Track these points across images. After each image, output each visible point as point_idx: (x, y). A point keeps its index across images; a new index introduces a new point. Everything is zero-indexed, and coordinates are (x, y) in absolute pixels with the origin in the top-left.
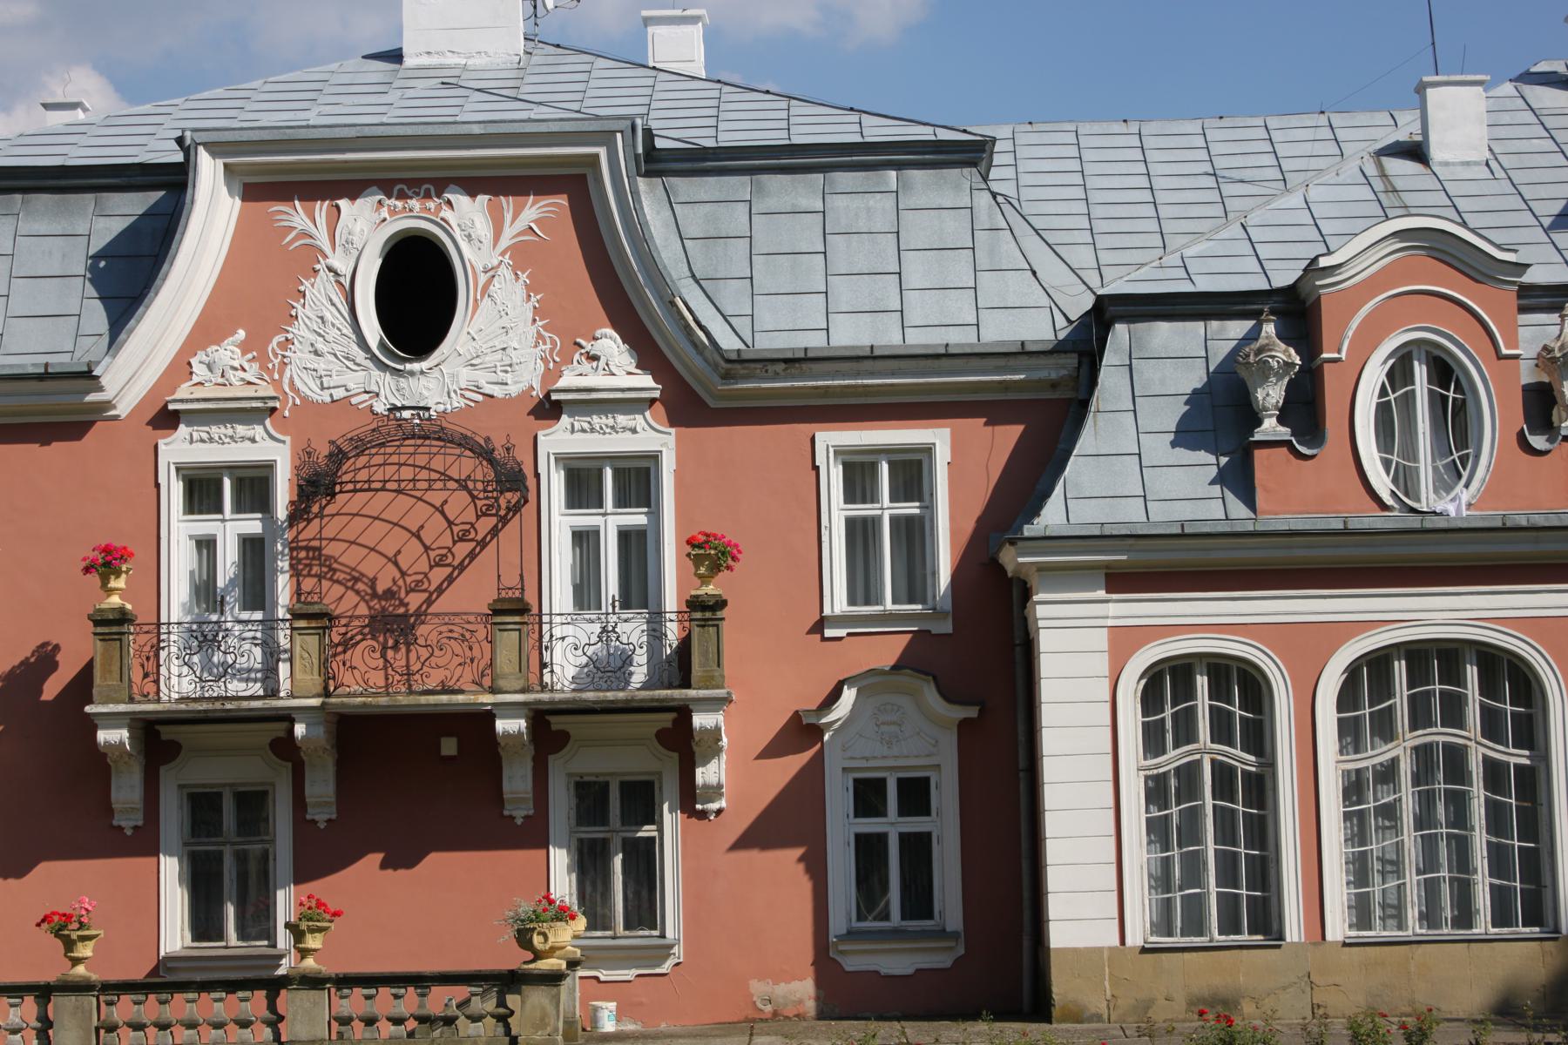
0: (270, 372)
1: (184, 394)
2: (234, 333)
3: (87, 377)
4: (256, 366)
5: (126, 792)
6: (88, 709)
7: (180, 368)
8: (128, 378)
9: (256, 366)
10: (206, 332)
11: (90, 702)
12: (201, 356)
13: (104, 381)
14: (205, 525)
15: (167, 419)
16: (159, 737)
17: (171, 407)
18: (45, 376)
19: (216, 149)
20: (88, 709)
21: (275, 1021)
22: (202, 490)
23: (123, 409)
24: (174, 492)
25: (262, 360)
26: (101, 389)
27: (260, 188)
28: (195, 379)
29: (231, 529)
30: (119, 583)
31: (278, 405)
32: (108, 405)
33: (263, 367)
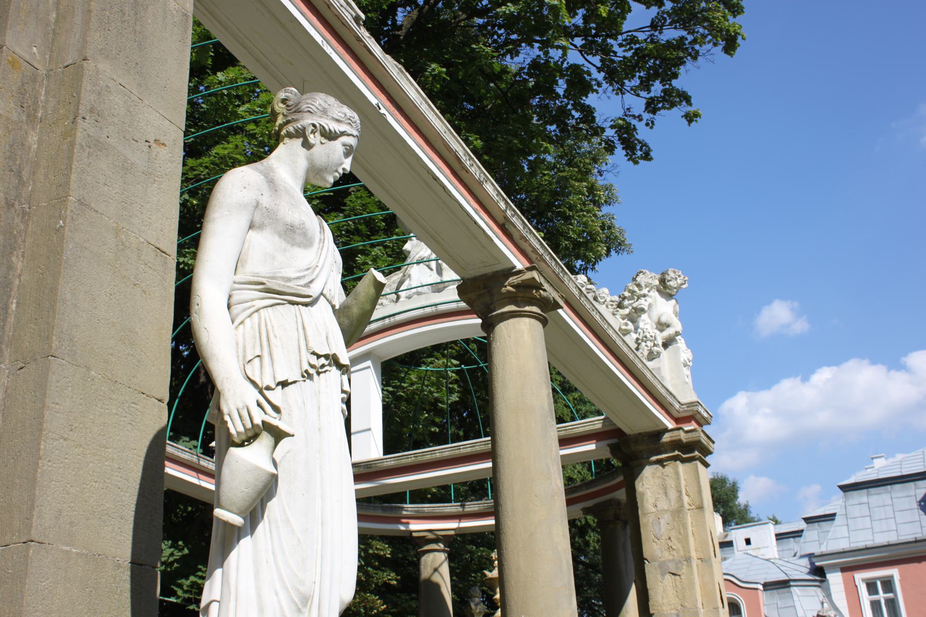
18: (916, 541)
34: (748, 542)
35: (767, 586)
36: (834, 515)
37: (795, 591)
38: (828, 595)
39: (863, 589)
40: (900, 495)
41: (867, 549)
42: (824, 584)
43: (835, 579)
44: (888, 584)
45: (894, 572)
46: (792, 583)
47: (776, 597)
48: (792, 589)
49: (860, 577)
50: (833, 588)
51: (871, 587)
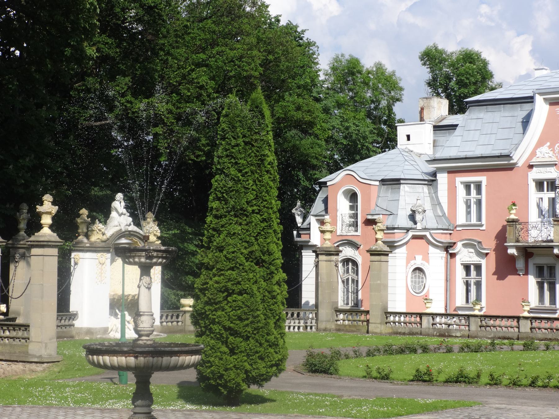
0: (555, 154)
1: (534, 161)
2: (546, 144)
3: (508, 157)
4: (552, 152)
5: (520, 264)
6: (505, 244)
7: (533, 154)
8: (520, 157)
9: (552, 152)
10: (540, 144)
11: (506, 242)
12: (539, 150)
13: (513, 158)
14: (541, 195)
15: (531, 167)
16: (528, 252)
17: (531, 164)
19: (541, 94)
20: (505, 244)
21: (519, 328)
22: (540, 185)
23: (520, 164)
24: (532, 186)
25: (553, 150)
26: (513, 160)
27: (553, 103)
28: (537, 156)
29: (547, 195)
30: (513, 212)
31: (557, 163)
32: (516, 164)
33: (554, 153)
34: (408, 137)
35: (384, 182)
36: (457, 125)
37: (404, 188)
38: (436, 192)
39: (461, 191)
40: (507, 114)
41: (466, 158)
42: (434, 182)
43: (442, 178)
44: (478, 187)
45: (482, 178)
46: (402, 182)
47: (387, 193)
48: (402, 186)
49: (460, 179)
50: (439, 186)
51: (467, 187)
